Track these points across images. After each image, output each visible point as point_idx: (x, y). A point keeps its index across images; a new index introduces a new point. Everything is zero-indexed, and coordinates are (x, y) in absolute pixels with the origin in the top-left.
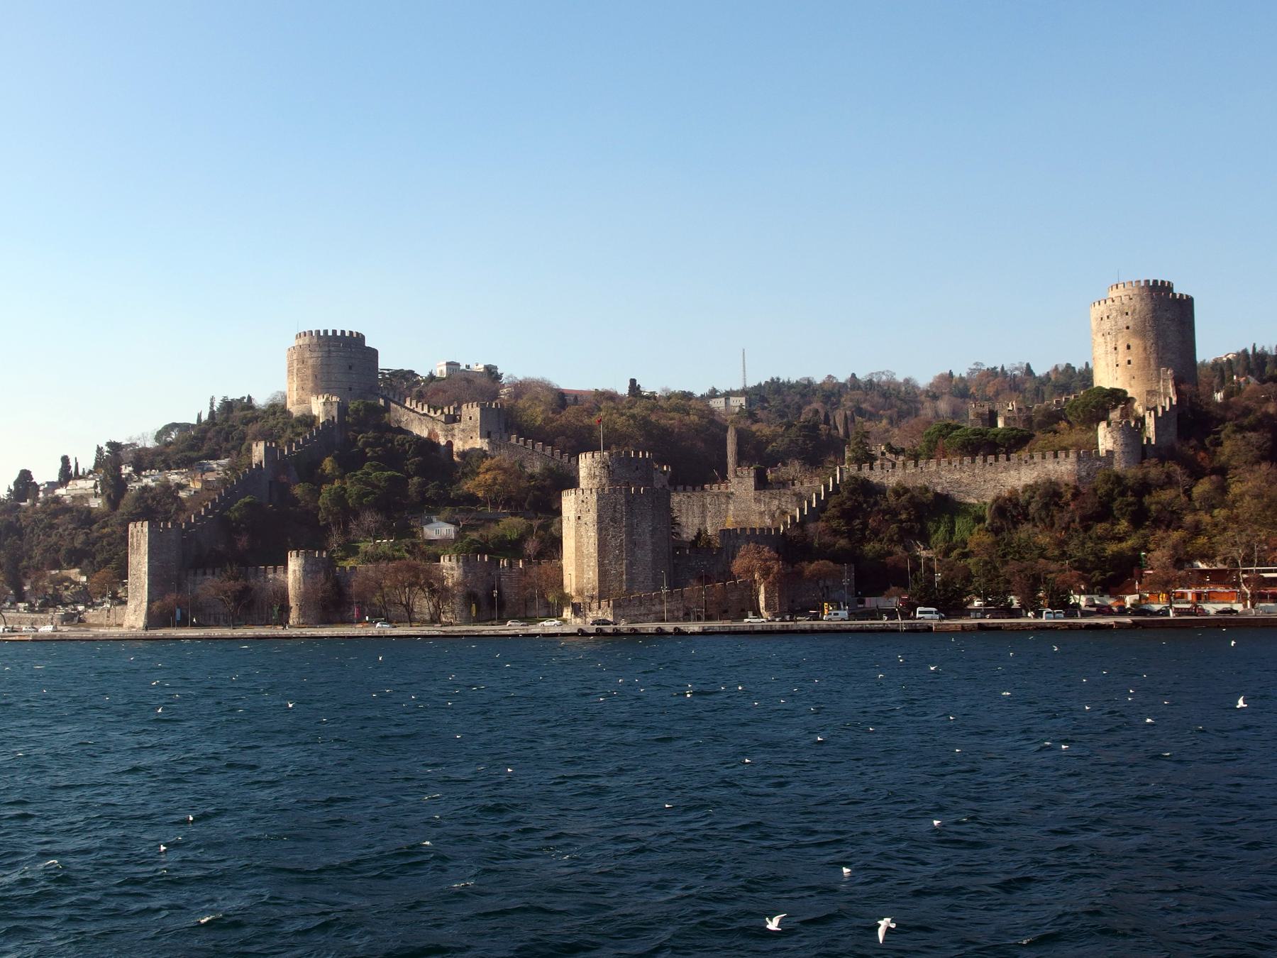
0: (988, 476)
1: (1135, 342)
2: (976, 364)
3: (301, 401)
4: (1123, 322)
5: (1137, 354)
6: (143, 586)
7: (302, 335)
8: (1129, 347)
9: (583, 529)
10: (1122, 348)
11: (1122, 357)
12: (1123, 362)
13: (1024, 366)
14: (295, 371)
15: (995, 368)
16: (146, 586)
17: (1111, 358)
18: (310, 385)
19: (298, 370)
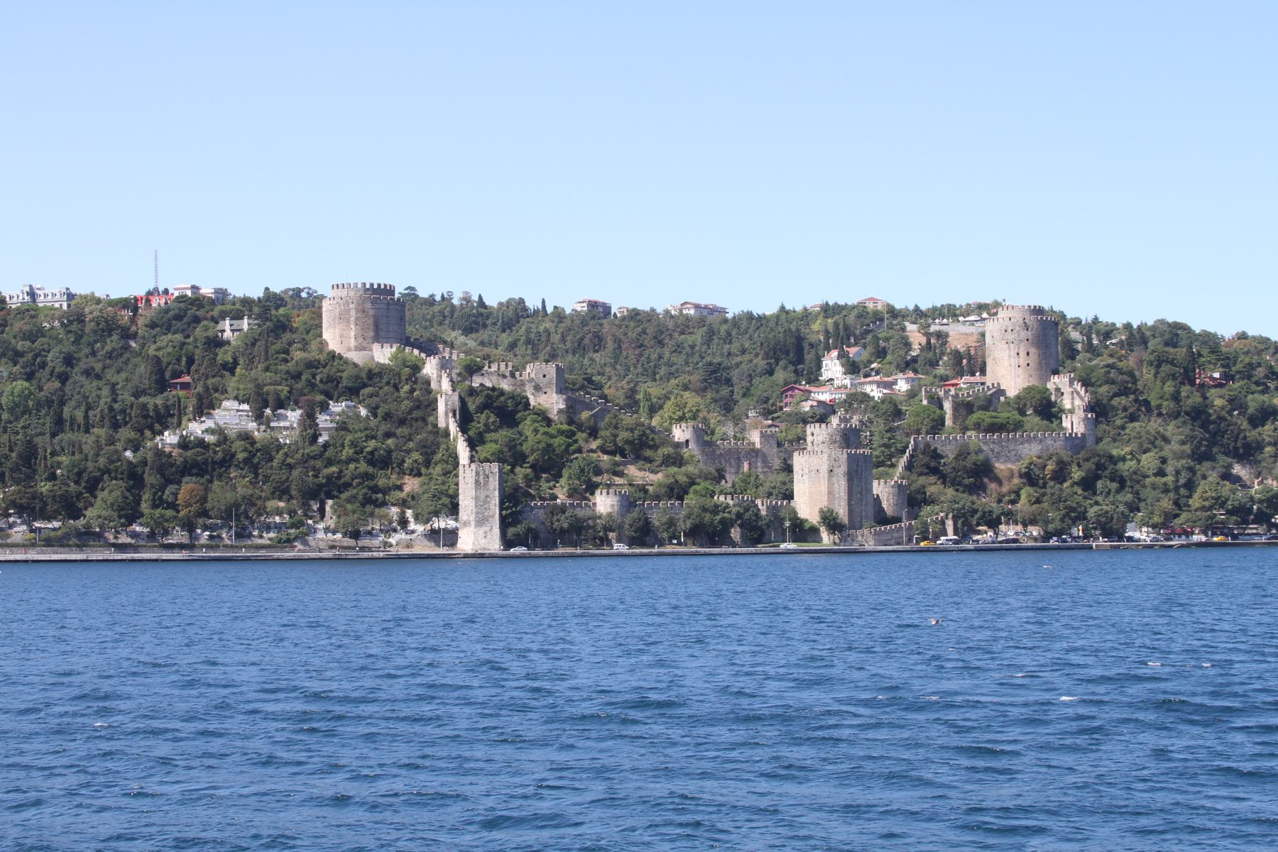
0: (1011, 447)
1: (1033, 351)
2: (409, 288)
3: (360, 348)
4: (1024, 334)
5: (1033, 359)
6: (493, 516)
7: (340, 286)
8: (1028, 354)
9: (834, 480)
10: (1023, 354)
11: (1023, 360)
12: (1023, 364)
13: (475, 298)
14: (353, 319)
15: (432, 296)
16: (497, 516)
17: (1014, 361)
18: (372, 334)
19: (357, 319)
